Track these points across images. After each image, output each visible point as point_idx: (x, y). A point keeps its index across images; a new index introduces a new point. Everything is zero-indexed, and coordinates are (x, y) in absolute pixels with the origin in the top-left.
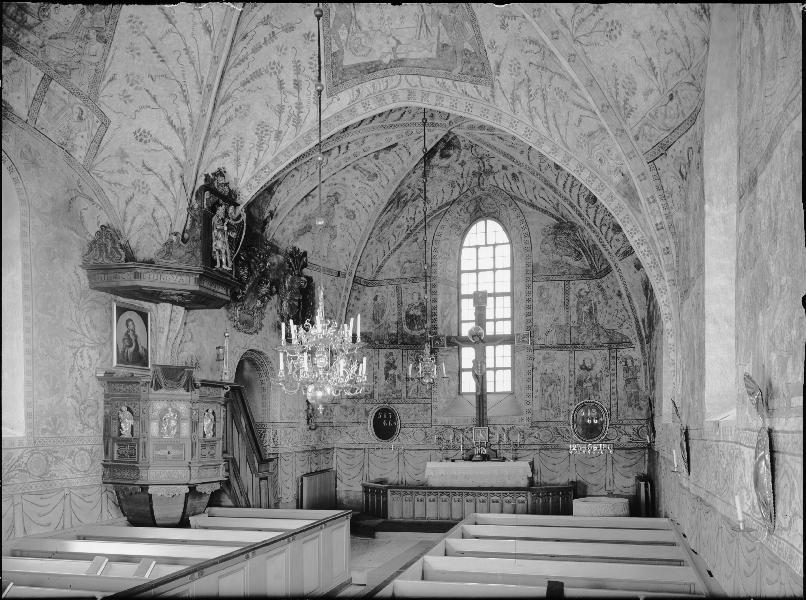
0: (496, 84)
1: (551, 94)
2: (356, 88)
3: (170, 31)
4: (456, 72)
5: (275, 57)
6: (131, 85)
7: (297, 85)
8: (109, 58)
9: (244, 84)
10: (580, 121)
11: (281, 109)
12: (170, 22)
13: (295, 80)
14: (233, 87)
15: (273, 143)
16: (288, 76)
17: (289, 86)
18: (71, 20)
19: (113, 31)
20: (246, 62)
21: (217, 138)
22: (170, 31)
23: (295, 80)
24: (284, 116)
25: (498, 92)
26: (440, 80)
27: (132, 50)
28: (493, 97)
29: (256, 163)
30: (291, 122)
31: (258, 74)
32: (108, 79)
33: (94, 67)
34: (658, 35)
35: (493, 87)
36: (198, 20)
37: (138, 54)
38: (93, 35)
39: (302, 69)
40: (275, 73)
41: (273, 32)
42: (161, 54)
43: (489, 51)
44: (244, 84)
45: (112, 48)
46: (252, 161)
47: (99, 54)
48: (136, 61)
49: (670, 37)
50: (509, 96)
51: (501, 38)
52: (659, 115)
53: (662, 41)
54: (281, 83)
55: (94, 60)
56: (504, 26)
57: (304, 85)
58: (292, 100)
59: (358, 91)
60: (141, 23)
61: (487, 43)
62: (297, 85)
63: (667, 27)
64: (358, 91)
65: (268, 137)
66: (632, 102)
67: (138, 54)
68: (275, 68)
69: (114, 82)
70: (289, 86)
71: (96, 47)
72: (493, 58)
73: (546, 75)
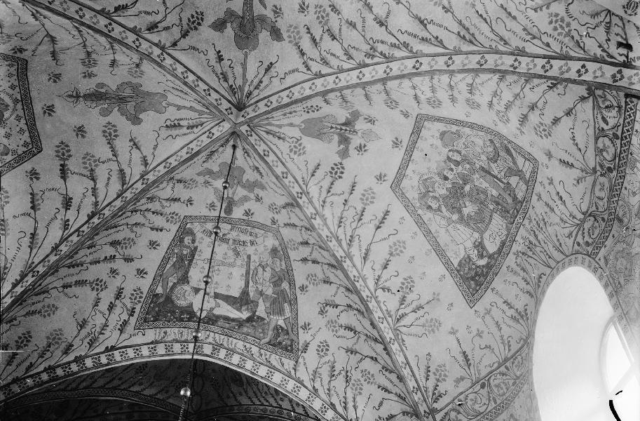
0: (301, 360)
1: (356, 375)
2: (164, 330)
4: (263, 341)
5: (105, 277)
7: (111, 307)
9: (65, 287)
10: (381, 404)
11: (82, 325)
12: (33, 208)
13: (111, 303)
14: (55, 284)
15: (58, 353)
16: (107, 296)
17: (103, 306)
20: (80, 268)
21: (9, 325)
23: (111, 303)
24: (84, 332)
25: (301, 368)
26: (248, 345)
28: (295, 370)
29: (28, 369)
30: (88, 340)
31: (80, 283)
34: (472, 335)
35: (296, 362)
39: (123, 297)
40: (97, 290)
41: (115, 256)
43: (301, 331)
44: (65, 287)
46: (27, 364)
49: (485, 335)
50: (311, 372)
51: (318, 322)
52: (468, 401)
53: (478, 338)
54: (97, 302)
56: (322, 312)
57: (117, 310)
58: (99, 320)
59: (165, 333)
61: (301, 323)
62: (111, 307)
63: (482, 328)
64: (165, 333)
65: (57, 346)
66: (441, 389)
68: (98, 285)
70: (103, 306)
72: (303, 337)
73: (354, 359)
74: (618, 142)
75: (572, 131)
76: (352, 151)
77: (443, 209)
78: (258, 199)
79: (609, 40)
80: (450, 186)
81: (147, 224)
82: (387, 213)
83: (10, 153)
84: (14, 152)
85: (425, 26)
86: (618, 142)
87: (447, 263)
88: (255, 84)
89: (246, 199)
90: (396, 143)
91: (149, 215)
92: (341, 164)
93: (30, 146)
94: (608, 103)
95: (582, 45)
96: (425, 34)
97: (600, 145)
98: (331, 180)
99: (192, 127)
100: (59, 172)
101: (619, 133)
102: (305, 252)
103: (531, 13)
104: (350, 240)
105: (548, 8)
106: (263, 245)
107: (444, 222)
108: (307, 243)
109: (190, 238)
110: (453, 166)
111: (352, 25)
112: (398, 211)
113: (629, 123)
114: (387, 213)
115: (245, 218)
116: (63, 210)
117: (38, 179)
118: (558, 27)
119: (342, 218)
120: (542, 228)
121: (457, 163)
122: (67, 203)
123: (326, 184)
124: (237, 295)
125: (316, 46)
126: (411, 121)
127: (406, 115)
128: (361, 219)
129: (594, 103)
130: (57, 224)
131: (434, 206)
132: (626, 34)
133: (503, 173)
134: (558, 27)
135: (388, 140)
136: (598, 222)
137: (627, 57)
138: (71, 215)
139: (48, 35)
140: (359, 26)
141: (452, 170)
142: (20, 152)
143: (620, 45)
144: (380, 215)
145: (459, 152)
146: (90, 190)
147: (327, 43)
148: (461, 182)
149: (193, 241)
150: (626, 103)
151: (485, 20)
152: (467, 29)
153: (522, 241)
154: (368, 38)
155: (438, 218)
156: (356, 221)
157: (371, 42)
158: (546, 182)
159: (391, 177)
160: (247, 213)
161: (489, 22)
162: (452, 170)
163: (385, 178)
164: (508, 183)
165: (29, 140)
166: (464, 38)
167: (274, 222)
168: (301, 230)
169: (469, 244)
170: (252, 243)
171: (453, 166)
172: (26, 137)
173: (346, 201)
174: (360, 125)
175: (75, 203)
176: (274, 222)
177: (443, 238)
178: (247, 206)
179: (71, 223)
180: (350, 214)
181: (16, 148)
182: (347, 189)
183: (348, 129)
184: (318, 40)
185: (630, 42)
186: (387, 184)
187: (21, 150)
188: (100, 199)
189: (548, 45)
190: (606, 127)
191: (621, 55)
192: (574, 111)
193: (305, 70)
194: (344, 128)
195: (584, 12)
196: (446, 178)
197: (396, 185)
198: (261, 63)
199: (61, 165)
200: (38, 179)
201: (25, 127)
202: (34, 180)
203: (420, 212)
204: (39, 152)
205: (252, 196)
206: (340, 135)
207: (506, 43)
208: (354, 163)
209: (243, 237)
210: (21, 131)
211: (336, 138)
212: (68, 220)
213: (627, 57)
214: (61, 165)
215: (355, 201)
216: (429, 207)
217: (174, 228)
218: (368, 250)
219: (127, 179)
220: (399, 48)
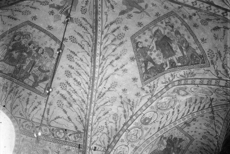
74: (64, 140)
75: (62, 118)
77: (14, 42)
79: (97, 145)
80: (26, 46)
85: (106, 79)
86: (64, 140)
90: (50, 27)
94: (76, 138)
95: (95, 135)
96: (104, 79)
97: (61, 131)
101: (67, 141)
103: (105, 121)
105: (106, 127)
110: (35, 49)
113: (71, 144)
118: (100, 128)
120: (16, 95)
121: (37, 51)
129: (75, 132)
131: (16, 38)
132: (98, 151)
133: (34, 72)
134: (100, 128)
135: (53, 24)
136: (32, 128)
137: (92, 149)
140: (113, 53)
143: (95, 148)
145: (42, 53)
147: (111, 37)
148: (28, 51)
150: (77, 144)
151: (104, 104)
152: (102, 96)
153: (5, 83)
155: (10, 40)
158: (38, 100)
161: (104, 105)
162: (34, 48)
164: (30, 75)
166: (100, 94)
171: (35, 49)
183: (64, 11)
185: (96, 151)
186: (30, 19)
189: (95, 124)
190: (68, 135)
191: (93, 147)
192: (70, 121)
195: (104, 139)
196: (30, 44)
198: (116, 3)
203: (13, 32)
206: (62, 7)
207: (97, 109)
211: (61, 5)
213: (92, 149)
216: (15, 36)
220: (102, 69)
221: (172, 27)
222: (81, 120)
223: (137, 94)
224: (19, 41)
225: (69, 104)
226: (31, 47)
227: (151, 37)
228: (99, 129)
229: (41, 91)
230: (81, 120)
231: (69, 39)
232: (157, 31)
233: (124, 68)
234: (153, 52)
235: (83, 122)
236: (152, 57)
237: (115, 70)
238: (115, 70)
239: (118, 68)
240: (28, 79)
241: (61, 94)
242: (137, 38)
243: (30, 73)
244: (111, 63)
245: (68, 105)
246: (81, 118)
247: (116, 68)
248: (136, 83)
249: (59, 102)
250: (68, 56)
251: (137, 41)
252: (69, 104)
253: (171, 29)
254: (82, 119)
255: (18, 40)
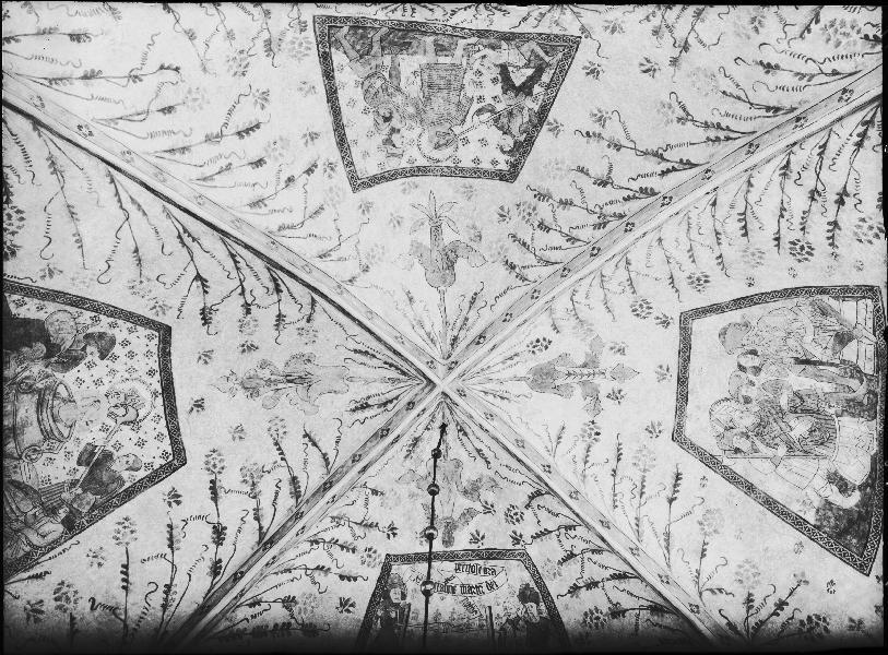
3: (164, 556)
6: (56, 599)
8: (60, 549)
12: (171, 546)
18: (54, 482)
19: (91, 522)
22: (164, 556)
27: (97, 558)
32: (31, 573)
33: (28, 549)
36: (210, 555)
37: (100, 565)
38: (62, 513)
42: (131, 579)
45: (73, 541)
47: (50, 538)
48: (90, 570)
55: (36, 540)
60: (132, 532)
67: (100, 565)
69: (40, 581)
71: (54, 528)
76: (606, 403)
77: (761, 447)
78: (489, 509)
80: (757, 409)
81: (334, 570)
82: (678, 477)
83: (143, 468)
84: (148, 466)
85: (661, 157)
87: (798, 523)
88: (458, 324)
89: (469, 514)
91: (336, 550)
92: (593, 422)
93: (171, 458)
96: (665, 166)
98: (584, 445)
99: (385, 404)
100: (209, 492)
102: (571, 572)
103: (798, 46)
104: (637, 525)
105: (817, 22)
106: (506, 586)
107: (767, 465)
108: (572, 555)
109: (398, 590)
110: (752, 377)
111: (566, 203)
112: (693, 468)
114: (678, 477)
115: (474, 547)
116: (213, 547)
117: (178, 503)
119: (615, 495)
121: (757, 370)
122: (219, 533)
123: (580, 451)
124: (517, 85)
125: (528, 249)
126: (675, 328)
127: (666, 323)
128: (642, 493)
130: (205, 566)
131: (744, 445)
133: (829, 352)
138: (224, 552)
139: (198, 277)
140: (577, 201)
141: (752, 383)
142: (156, 466)
144: (670, 481)
145: (754, 353)
146: (252, 512)
147: (542, 239)
149: (404, 596)
151: (739, 98)
152: (719, 126)
154: (591, 207)
155: (757, 463)
156: (638, 496)
157: (597, 210)
159: (669, 423)
160: (475, 539)
161: (744, 97)
162: (752, 383)
163: (661, 428)
165: (169, 450)
166: (718, 139)
167: (517, 539)
168: (558, 536)
169: (820, 482)
170: (491, 586)
171: (752, 377)
172: (166, 445)
173: (614, 471)
174: (608, 361)
175: (230, 533)
176: (517, 539)
177: (777, 491)
178: (472, 527)
179: (223, 564)
180: (624, 487)
181: (150, 460)
182: (612, 455)
184: (529, 242)
187: (157, 464)
188: (265, 524)
189: (835, 73)
193: (520, 283)
194: (585, 371)
196: (747, 400)
197: (678, 436)
199: (211, 482)
200: (178, 503)
201: (166, 432)
202: (174, 504)
204: (184, 465)
205: (478, 506)
208: (612, 417)
209: (474, 580)
210: (159, 437)
211: (578, 391)
212: (220, 561)
214: (211, 482)
215: (626, 468)
216: (737, 450)
217: (375, 573)
218: (668, 535)
219: (302, 489)
220: (635, 197)
221: (388, 141)
222: (867, 130)
223: (613, 31)
224: (750, 434)
225: (841, 202)
226: (753, 393)
227: (466, 141)
228: (844, 41)
229: (871, 308)
230: (867, 130)
231: (653, 316)
232: (438, 146)
233: (597, 128)
234: (489, 101)
235: (868, 118)
236: (498, 89)
237: (618, 147)
238: (618, 147)
239: (609, 146)
240: (861, 364)
241: (831, 244)
242: (503, 166)
243: (838, 362)
244: (603, 183)
245: (849, 201)
246: (858, 135)
247: (612, 151)
248: (597, 60)
249: (863, 238)
250: (700, 287)
251: (506, 157)
252: (841, 202)
253: (395, 138)
254: (861, 129)
255: (748, 437)
